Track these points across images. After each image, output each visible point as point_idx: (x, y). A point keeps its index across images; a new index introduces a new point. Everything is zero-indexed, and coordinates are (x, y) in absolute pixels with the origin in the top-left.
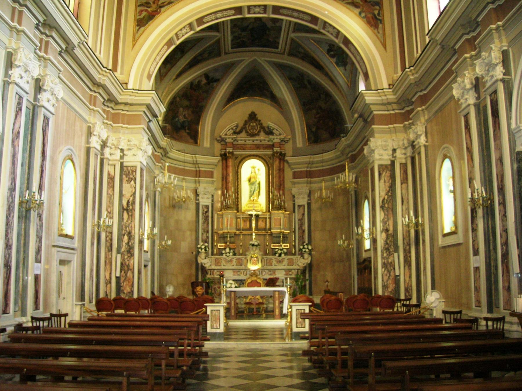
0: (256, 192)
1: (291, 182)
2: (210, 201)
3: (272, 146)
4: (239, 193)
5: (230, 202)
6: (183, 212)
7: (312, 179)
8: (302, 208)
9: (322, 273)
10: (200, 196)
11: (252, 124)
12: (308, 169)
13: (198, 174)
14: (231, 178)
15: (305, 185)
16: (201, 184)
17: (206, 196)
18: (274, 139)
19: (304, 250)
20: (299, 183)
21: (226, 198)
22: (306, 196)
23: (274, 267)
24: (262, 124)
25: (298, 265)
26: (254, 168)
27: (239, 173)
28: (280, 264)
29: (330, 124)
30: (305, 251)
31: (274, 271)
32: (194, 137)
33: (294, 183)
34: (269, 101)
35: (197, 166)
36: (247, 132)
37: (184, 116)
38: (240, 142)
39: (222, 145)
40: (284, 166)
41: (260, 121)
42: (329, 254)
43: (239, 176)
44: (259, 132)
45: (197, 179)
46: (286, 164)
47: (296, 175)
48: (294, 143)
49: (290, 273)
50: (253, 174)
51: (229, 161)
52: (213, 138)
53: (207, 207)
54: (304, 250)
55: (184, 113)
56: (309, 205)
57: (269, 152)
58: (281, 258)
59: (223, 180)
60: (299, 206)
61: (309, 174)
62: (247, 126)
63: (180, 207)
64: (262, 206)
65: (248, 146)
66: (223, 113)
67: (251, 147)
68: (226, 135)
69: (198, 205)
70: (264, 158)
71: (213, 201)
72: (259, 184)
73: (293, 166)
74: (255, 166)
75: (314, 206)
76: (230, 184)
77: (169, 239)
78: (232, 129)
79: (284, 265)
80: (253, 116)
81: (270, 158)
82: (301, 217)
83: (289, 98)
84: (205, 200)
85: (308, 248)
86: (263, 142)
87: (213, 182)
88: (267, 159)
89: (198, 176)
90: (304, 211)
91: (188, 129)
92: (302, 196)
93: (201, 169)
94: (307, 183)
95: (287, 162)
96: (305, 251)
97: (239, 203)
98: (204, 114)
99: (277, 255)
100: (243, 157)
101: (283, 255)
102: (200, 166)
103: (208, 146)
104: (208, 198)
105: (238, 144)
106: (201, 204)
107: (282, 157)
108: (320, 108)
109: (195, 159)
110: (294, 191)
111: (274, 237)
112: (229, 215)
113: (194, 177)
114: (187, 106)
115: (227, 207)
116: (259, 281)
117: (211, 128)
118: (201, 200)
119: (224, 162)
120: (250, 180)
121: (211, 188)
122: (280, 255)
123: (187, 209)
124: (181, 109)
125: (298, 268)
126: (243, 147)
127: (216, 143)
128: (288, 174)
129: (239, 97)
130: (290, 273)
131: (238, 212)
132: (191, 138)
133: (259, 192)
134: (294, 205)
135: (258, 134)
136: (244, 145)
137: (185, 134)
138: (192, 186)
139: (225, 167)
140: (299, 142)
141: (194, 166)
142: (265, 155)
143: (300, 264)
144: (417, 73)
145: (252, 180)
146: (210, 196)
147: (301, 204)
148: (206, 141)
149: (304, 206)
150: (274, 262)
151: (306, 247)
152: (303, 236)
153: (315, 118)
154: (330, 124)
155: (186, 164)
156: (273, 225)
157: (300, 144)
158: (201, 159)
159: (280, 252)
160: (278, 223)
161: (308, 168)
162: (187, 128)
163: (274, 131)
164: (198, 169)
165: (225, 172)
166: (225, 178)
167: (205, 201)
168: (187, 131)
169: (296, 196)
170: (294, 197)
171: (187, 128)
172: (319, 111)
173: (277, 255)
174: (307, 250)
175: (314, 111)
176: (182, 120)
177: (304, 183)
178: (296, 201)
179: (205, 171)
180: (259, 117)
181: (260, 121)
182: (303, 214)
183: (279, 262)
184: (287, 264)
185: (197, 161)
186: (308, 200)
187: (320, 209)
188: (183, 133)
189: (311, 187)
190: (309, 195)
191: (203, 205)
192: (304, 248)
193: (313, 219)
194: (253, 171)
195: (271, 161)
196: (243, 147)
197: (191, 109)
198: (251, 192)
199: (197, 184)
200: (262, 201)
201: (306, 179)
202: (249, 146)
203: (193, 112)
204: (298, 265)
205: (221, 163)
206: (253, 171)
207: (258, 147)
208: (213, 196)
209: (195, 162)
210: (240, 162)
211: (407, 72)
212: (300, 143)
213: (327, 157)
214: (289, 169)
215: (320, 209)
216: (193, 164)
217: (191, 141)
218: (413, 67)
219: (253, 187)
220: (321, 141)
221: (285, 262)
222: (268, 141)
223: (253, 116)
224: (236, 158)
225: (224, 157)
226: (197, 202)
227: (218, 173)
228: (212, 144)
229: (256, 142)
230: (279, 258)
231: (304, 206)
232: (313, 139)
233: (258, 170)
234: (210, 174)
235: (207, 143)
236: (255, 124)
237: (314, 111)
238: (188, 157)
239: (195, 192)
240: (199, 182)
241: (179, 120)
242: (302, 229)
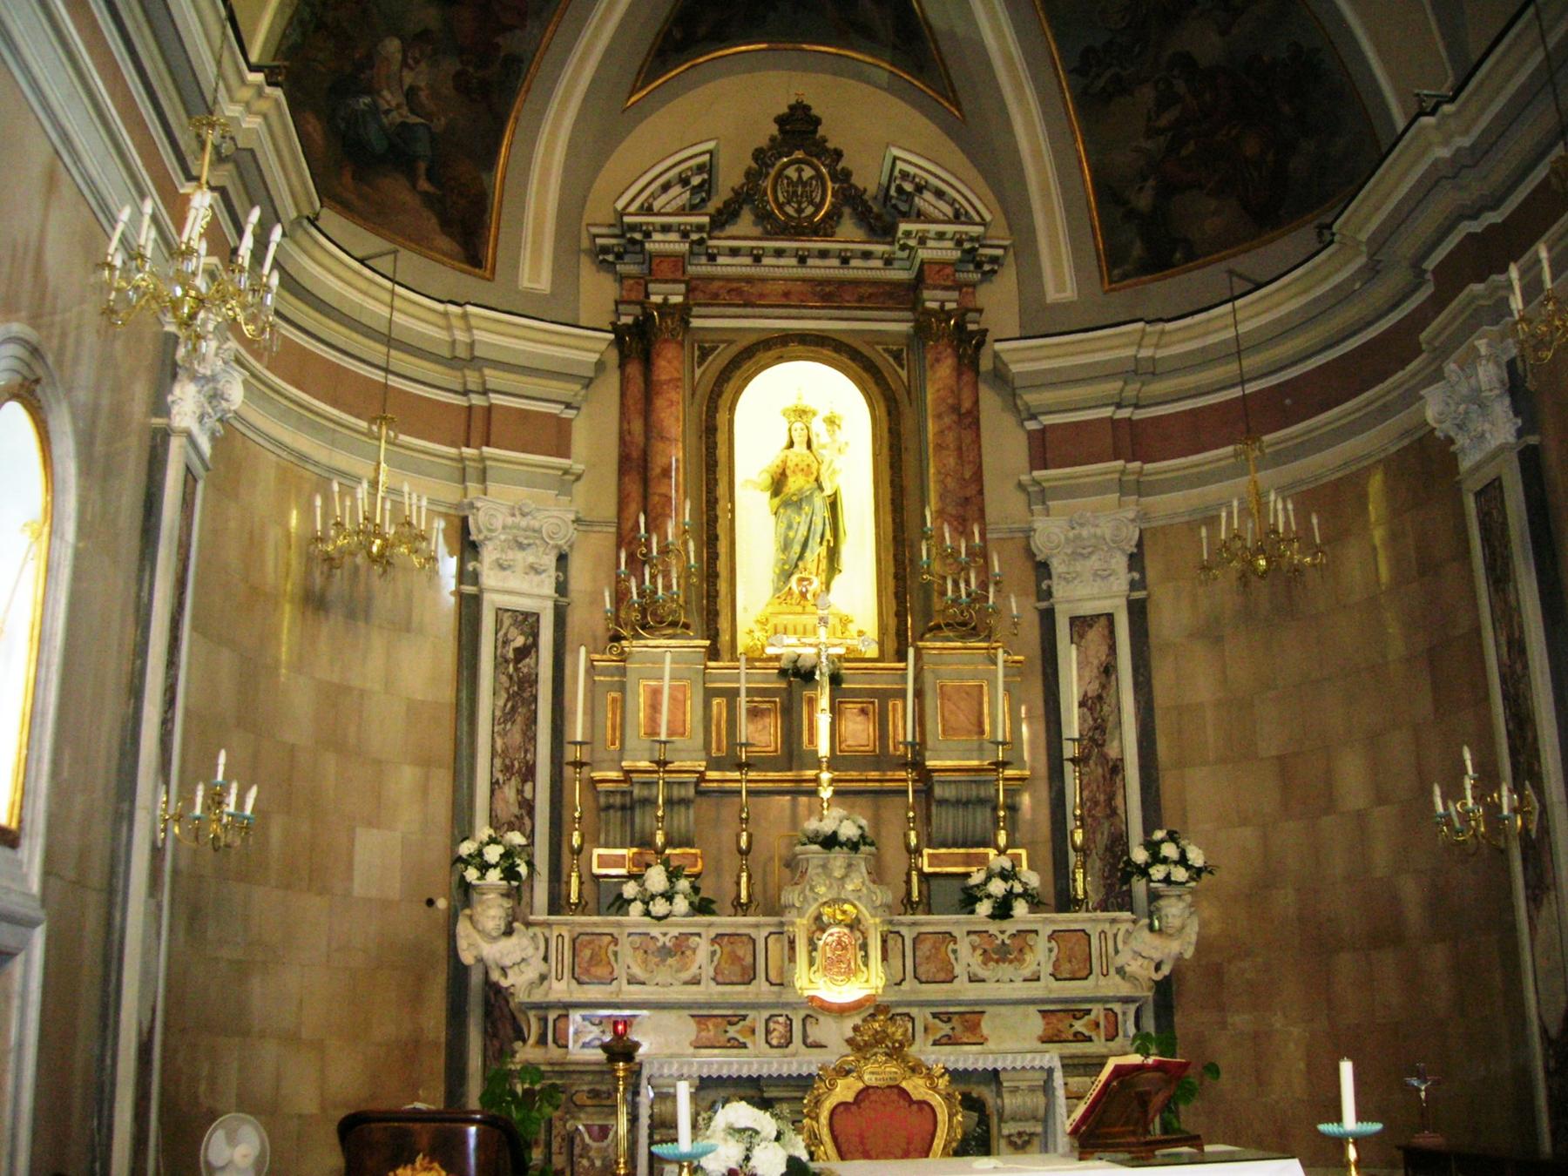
0: (817, 551)
1: (1021, 486)
2: (549, 589)
3: (905, 295)
4: (722, 548)
5: (671, 584)
6: (378, 642)
7: (1149, 467)
8: (1094, 635)
9: (1241, 1020)
10: (489, 554)
11: (791, 172)
12: (1124, 413)
13: (478, 426)
14: (675, 455)
15: (1114, 497)
16: (492, 487)
17: (522, 558)
18: (922, 241)
19: (1158, 872)
20: (1072, 492)
21: (647, 559)
22: (1120, 563)
23: (972, 992)
24: (847, 174)
25: (1120, 971)
26: (802, 413)
27: (721, 437)
28: (1006, 970)
29: (1251, 147)
30: (1167, 880)
31: (964, 1023)
32: (463, 226)
33: (1039, 496)
34: (882, 69)
35: (472, 379)
36: (763, 217)
37: (411, 94)
38: (727, 265)
39: (621, 278)
40: (976, 402)
41: (838, 154)
42: (1285, 900)
43: (722, 452)
44: (834, 216)
45: (468, 451)
46: (990, 401)
47: (1046, 448)
48: (1030, 278)
49: (1079, 1026)
50: (800, 447)
51: (667, 355)
52: (572, 243)
53: (528, 622)
54: (1158, 872)
55: (408, 78)
56: (1138, 611)
57: (898, 326)
58: (1010, 927)
59: (622, 471)
60: (1080, 624)
61: (1133, 441)
62: (767, 184)
63: (358, 610)
64: (853, 629)
65: (769, 287)
66: (632, 116)
67: (786, 295)
68: (647, 210)
69: (469, 607)
70: (865, 350)
71: (562, 588)
72: (833, 505)
73: (1031, 398)
74: (806, 403)
75: (1169, 619)
76: (665, 495)
77: (246, 774)
78: (684, 182)
79: (1035, 975)
80: (798, 127)
81: (897, 356)
82: (1094, 689)
83: (1000, 36)
84: (515, 581)
85: (1183, 860)
86: (859, 270)
87: (566, 482)
88: (885, 361)
89: (476, 435)
90: (1112, 649)
91: (429, 179)
92: (1094, 562)
93: (496, 399)
94: (1123, 488)
95: (1001, 377)
96: (1167, 880)
97: (723, 603)
98: (522, 107)
99: (984, 908)
100: (745, 342)
101: (1020, 908)
102: (494, 377)
103: (544, 284)
104: (535, 570)
105: (711, 278)
106: (490, 602)
107: (967, 343)
108: (1186, 62)
109: (461, 336)
110: (1049, 531)
111: (942, 802)
112: (665, 658)
113: (453, 444)
114: (424, 36)
115: (651, 619)
116: (917, 1087)
117: (565, 187)
118: (490, 578)
119: (634, 369)
120: (778, 484)
121: (555, 517)
122: (1003, 909)
123: (404, 625)
124: (393, 46)
125: (1125, 989)
126: (739, 292)
127: (587, 269)
128: (1004, 445)
129: (721, 37)
130: (1079, 1026)
131: (713, 653)
132: (446, 224)
133: (833, 554)
134: (1048, 618)
135: (823, 229)
136: (749, 280)
137: (406, 197)
138: (449, 492)
139: (640, 403)
140: (1058, 276)
141: (450, 378)
142: (877, 338)
143: (1134, 967)
144: (1466, 132)
145: (794, 483)
146: (550, 561)
147: (1087, 609)
148: (532, 250)
149: (1110, 617)
150: (966, 957)
151: (1169, 850)
152: (1111, 798)
153: (1151, 133)
154: (1251, 147)
155: (400, 360)
156: (935, 726)
157: (1060, 287)
158: (495, 333)
159: (997, 887)
160: (962, 719)
161: (1119, 406)
162: (422, 166)
163: (925, 202)
164: (477, 400)
165: (637, 426)
166: (637, 467)
167: (516, 585)
168: (424, 185)
169: (1057, 566)
170: (1042, 569)
171: (422, 166)
172: (1180, 87)
173: (984, 908)
174: (1180, 874)
175: (1146, 95)
176: (395, 117)
177: (1100, 489)
178: (1059, 590)
179: (524, 415)
180: (833, 133)
181: (838, 154)
182: (1108, 670)
183: (1000, 954)
184: (1047, 969)
185: (472, 345)
186: (1133, 585)
187: (1210, 633)
188: (396, 189)
189: (1143, 516)
190: (1136, 561)
191: (500, 611)
192: (1156, 858)
193: (1161, 697)
194: (803, 422)
195: (904, 374)
196: (742, 294)
197: (450, 65)
198: (786, 546)
199: (473, 487)
200: (855, 601)
201: (1120, 463)
202: (780, 287)
203: (462, 83)
204: (1120, 971)
205: (612, 380)
206: (803, 422)
207: (830, 294)
208: (562, 559)
209: (462, 352)
210: (724, 376)
211: (1423, 128)
212: (1061, 273)
213: (1261, 314)
214: (1008, 421)
215: (1210, 633)
216: (453, 362)
217: (444, 243)
218: (1452, 100)
219: (801, 522)
220: (1190, 256)
221: (1040, 955)
222: (888, 262)
223: (798, 127)
224: (704, 354)
225: (637, 341)
226: (469, 589)
227: (595, 434)
228: (564, 271)
229: (819, 269)
230: (993, 927)
231: (1110, 617)
232: (1137, 250)
233: (831, 421)
234: (556, 437)
235: (535, 270)
236: (808, 173)
237: (1146, 95)
238: (418, 317)
239: (456, 536)
240: (483, 477)
241: (374, 108)
242: (1104, 757)
